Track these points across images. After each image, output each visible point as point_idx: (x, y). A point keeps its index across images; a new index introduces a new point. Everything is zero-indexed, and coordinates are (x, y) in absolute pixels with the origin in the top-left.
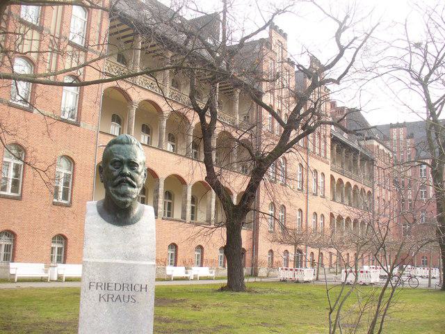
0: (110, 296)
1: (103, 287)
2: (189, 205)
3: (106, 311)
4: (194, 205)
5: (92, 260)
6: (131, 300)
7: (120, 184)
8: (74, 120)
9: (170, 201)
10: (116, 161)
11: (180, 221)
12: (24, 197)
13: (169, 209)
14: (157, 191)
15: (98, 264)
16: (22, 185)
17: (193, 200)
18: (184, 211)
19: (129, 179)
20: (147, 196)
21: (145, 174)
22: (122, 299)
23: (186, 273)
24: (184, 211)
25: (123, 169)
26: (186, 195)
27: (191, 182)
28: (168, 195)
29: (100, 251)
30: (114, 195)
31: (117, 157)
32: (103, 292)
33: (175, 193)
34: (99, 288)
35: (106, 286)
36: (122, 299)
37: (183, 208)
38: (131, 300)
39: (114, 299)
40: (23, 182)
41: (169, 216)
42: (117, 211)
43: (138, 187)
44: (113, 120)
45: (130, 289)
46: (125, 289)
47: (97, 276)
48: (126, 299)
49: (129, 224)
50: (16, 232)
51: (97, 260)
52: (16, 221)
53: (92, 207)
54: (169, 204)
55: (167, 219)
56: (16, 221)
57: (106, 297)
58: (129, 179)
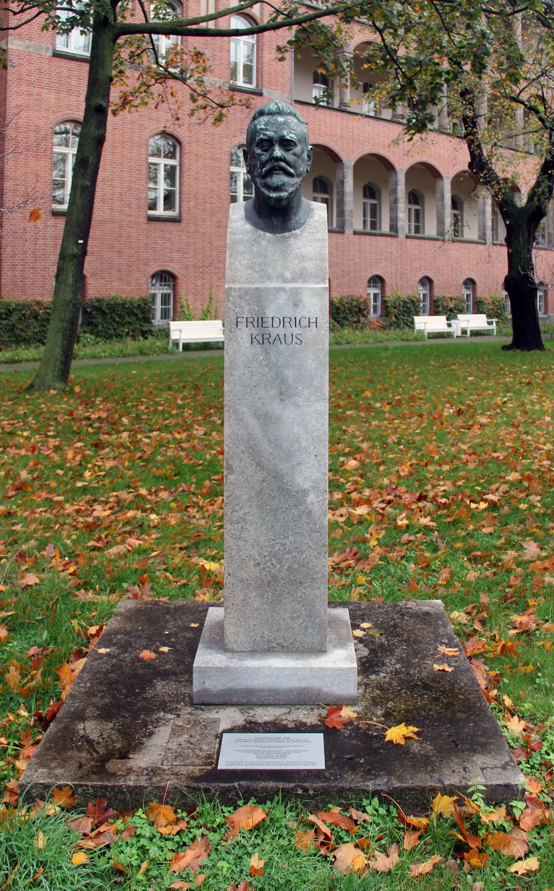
0: (265, 336)
1: (255, 324)
2: (448, 211)
3: (261, 358)
4: (456, 212)
5: (237, 286)
6: (295, 340)
7: (269, 173)
8: (253, 86)
9: (418, 207)
10: (262, 140)
11: (437, 240)
12: (185, 216)
13: (417, 220)
14: (394, 191)
15: (247, 292)
16: (180, 198)
17: (456, 204)
18: (441, 222)
19: (283, 164)
20: (423, 206)
21: (309, 156)
22: (283, 340)
23: (449, 325)
24: (441, 222)
25: (274, 150)
26: (443, 197)
27: (448, 173)
28: (414, 198)
29: (250, 271)
30: (266, 192)
31: (264, 135)
32: (255, 332)
33: (463, 198)
34: (250, 325)
35: (260, 321)
36: (283, 340)
37: (438, 218)
38: (295, 340)
39: (272, 341)
40: (180, 193)
41: (417, 230)
42: (274, 214)
43: (298, 176)
44: (316, 81)
45: (293, 326)
46: (287, 324)
47: (246, 309)
48: (289, 340)
49: (289, 230)
50: (176, 272)
51: (246, 286)
52: (175, 256)
53: (238, 213)
54: (417, 212)
55: (453, 241)
56: (175, 256)
57: (259, 338)
58: (283, 164)
